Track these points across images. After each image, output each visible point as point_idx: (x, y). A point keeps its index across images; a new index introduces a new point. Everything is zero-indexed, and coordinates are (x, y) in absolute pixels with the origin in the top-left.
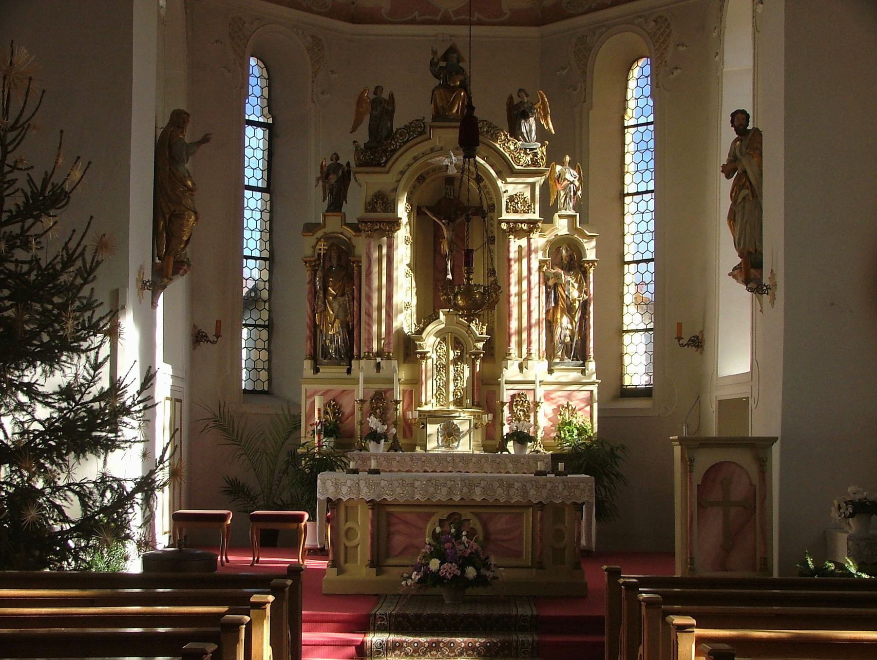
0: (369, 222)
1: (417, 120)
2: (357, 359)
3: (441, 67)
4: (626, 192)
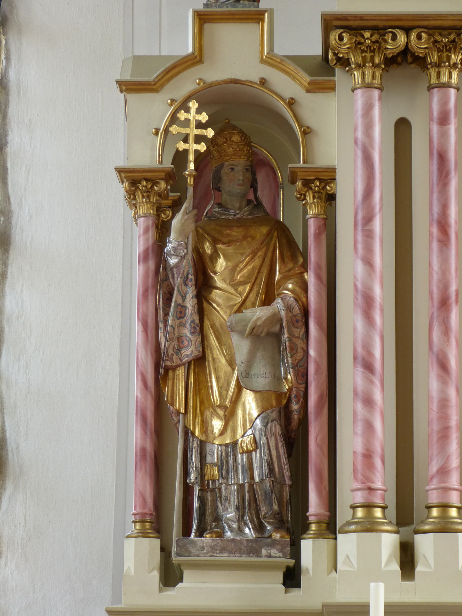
0: (365, 28)
2: (319, 535)
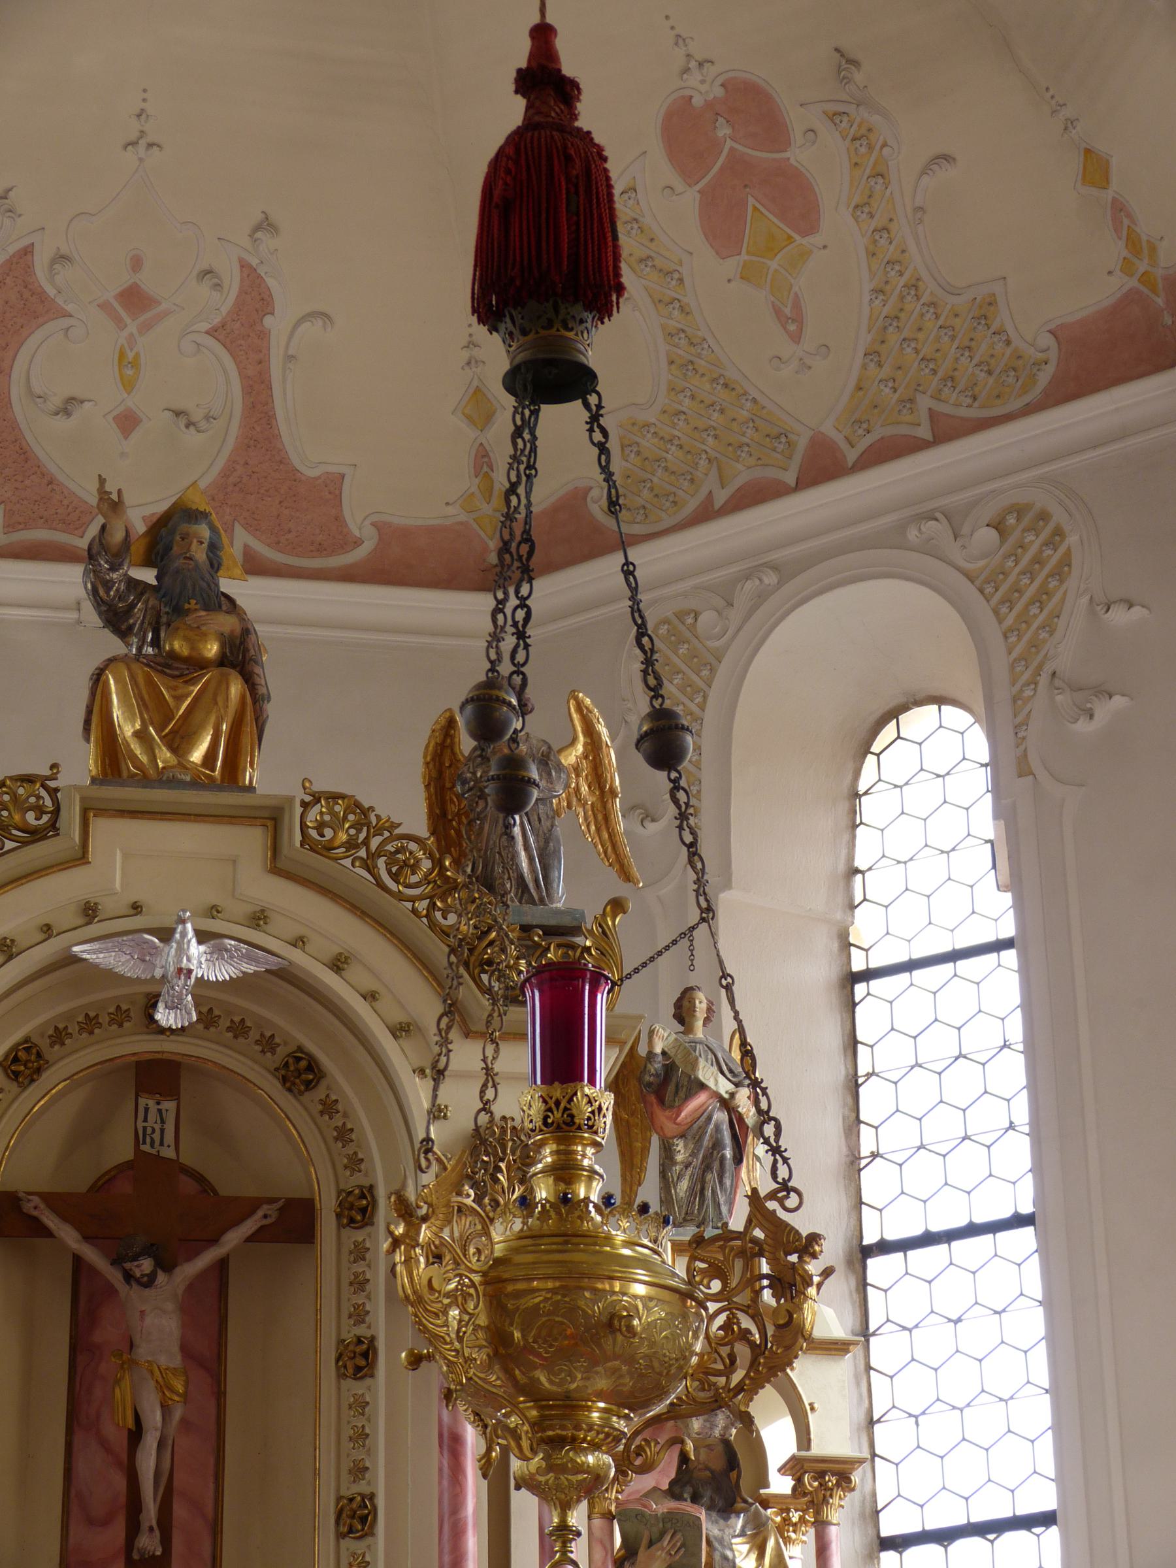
1: (28, 779)
3: (133, 584)
4: (870, 1238)
